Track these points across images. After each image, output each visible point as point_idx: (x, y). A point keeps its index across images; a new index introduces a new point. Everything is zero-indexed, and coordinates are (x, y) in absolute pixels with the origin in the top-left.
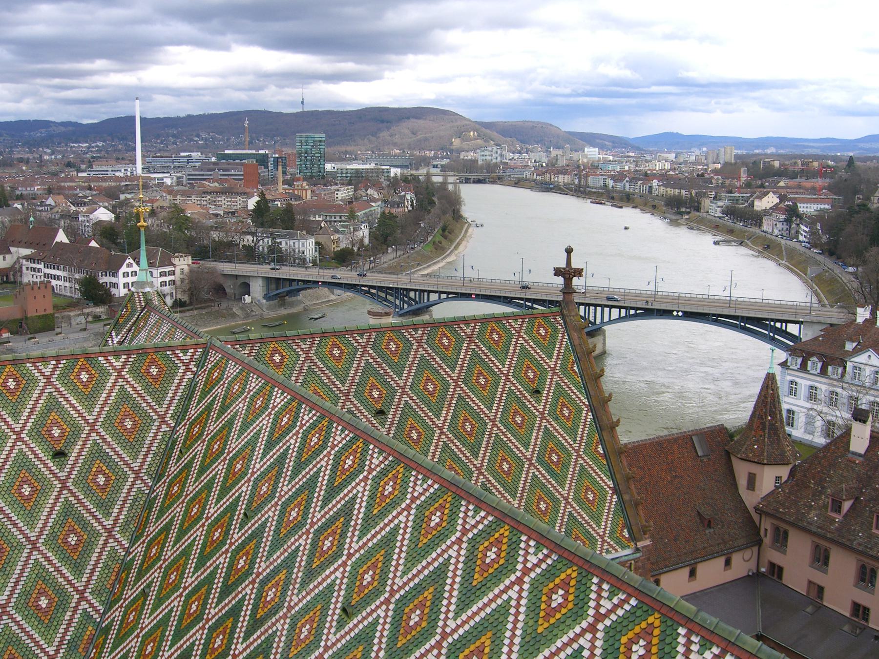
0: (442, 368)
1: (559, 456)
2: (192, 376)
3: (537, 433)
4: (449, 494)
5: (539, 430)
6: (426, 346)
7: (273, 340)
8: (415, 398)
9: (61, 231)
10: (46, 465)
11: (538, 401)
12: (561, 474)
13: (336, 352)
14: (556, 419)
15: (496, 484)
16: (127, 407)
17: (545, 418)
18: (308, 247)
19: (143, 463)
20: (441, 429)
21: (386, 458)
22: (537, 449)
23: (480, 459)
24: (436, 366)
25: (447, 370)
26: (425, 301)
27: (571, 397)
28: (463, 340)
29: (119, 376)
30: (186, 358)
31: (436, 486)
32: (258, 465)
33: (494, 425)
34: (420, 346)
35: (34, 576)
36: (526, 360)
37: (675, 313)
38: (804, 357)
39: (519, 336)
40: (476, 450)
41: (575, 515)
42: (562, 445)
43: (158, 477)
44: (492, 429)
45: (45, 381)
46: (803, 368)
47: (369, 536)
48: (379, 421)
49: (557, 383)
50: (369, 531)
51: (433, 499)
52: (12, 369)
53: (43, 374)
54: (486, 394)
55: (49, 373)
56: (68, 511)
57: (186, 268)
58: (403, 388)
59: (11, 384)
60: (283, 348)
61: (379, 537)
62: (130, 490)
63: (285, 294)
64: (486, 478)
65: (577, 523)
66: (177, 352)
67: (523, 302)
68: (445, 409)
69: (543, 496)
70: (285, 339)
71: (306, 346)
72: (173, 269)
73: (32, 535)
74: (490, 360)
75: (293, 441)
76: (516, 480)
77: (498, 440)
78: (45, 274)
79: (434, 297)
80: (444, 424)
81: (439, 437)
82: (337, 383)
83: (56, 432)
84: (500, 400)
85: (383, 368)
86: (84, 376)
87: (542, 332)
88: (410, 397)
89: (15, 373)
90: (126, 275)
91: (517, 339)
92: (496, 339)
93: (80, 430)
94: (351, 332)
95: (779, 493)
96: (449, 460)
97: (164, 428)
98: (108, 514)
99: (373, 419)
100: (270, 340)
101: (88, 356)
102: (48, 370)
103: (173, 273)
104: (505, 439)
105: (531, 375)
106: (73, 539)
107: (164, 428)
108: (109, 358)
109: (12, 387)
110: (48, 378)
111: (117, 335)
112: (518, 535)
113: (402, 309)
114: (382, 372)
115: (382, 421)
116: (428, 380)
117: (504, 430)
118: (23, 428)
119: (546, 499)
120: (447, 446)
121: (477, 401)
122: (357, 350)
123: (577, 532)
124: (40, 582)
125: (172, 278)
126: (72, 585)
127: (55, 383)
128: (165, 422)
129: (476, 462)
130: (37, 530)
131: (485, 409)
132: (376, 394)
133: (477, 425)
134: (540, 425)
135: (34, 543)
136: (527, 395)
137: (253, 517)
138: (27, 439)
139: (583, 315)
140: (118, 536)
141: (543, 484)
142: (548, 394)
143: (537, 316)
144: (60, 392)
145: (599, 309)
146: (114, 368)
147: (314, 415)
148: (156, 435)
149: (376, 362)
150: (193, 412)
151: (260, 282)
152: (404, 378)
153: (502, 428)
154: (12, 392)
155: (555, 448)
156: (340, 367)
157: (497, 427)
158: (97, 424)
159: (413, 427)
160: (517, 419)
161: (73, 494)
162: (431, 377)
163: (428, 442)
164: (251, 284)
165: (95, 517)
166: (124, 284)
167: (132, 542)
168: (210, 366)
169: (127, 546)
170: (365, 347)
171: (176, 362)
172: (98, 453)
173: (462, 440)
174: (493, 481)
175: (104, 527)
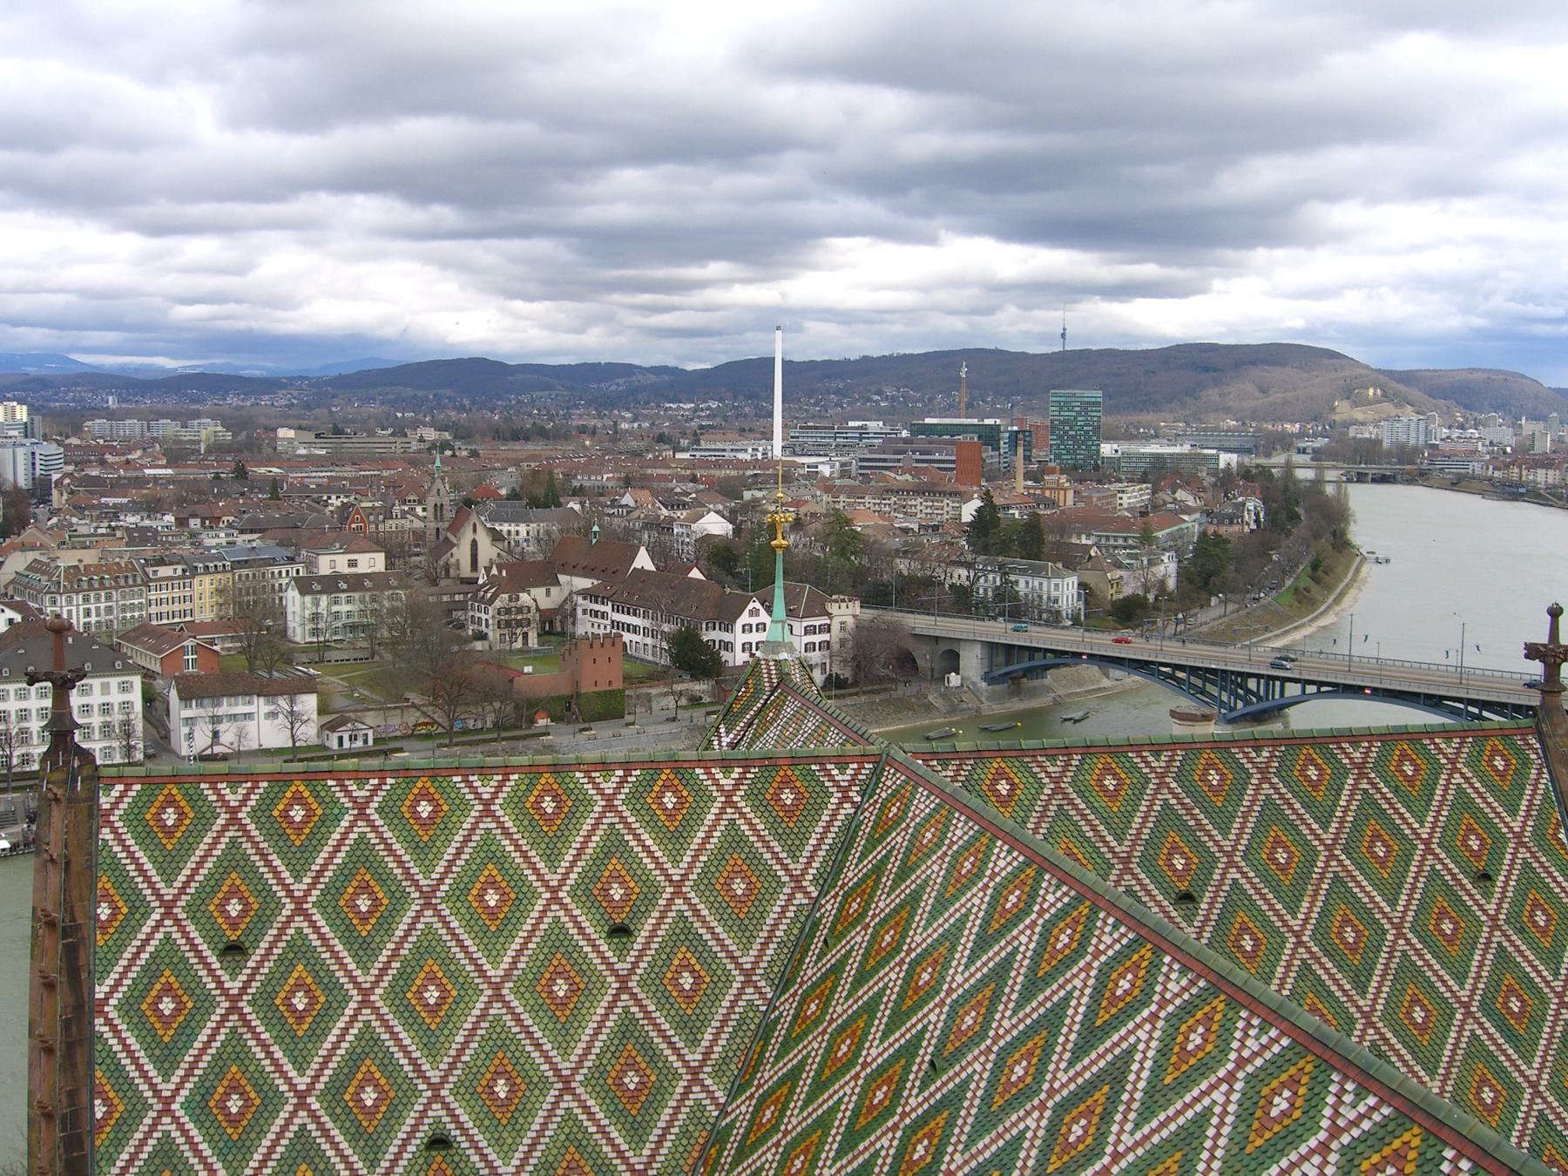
1: (1523, 1001)
2: (852, 811)
3: (1483, 956)
4: (1309, 1058)
5: (1485, 950)
6: (1275, 780)
7: (997, 754)
8: (1251, 874)
9: (643, 549)
10: (596, 948)
11: (1487, 895)
12: (1527, 1037)
13: (1110, 782)
14: (1521, 931)
15: (1398, 1046)
16: (738, 857)
17: (1499, 928)
18: (1065, 590)
19: (759, 957)
20: (1297, 935)
21: (1193, 983)
22: (1481, 986)
23: (1370, 996)
24: (1294, 817)
25: (1315, 826)
26: (1277, 696)
27: (1551, 891)
28: (1347, 771)
29: (729, 802)
30: (843, 779)
31: (1285, 1042)
32: (960, 978)
33: (1400, 935)
34: (1264, 779)
35: (563, 1137)
36: (1467, 815)
39: (1455, 769)
40: (1363, 979)
41: (1551, 1117)
42: (1531, 980)
43: (784, 983)
44: (1394, 942)
45: (604, 803)
47: (1154, 1124)
48: (1182, 913)
50: (1154, 1114)
51: (1277, 1064)
52: (551, 781)
53: (601, 792)
54: (1386, 876)
55: (611, 791)
56: (627, 1029)
57: (850, 621)
58: (1229, 855)
59: (548, 805)
60: (1015, 770)
61: (1173, 1127)
62: (734, 1003)
63: (1021, 674)
64: (1380, 1034)
65: (1553, 1134)
66: (829, 767)
67: (1462, 706)
68: (1307, 899)
69: (1490, 1076)
70: (1019, 753)
71: (1056, 769)
73: (565, 1067)
74: (1396, 811)
75: (1024, 939)
76: (1438, 1041)
77: (1407, 964)
79: (1292, 690)
80: (1303, 926)
81: (1294, 950)
82: (1109, 838)
83: (617, 893)
84: (1413, 888)
85: (1194, 817)
86: (669, 800)
87: (1499, 763)
88: (1242, 873)
89: (555, 786)
90: (747, 628)
91: (1450, 776)
92: (1410, 773)
93: (658, 891)
94: (1138, 748)
96: (1311, 995)
97: (800, 899)
98: (694, 1042)
99: (1171, 908)
100: (992, 754)
101: (677, 765)
102: (610, 785)
103: (828, 629)
104: (1420, 963)
105: (1474, 844)
106: (632, 1080)
107: (800, 899)
108: (713, 771)
109: (549, 810)
110: (609, 799)
111: (728, 733)
112: (1439, 1147)
113: (1232, 709)
114: (1192, 823)
115: (1189, 913)
116: (1277, 842)
117: (1419, 946)
118: (562, 883)
119: (1494, 1082)
120: (1308, 967)
121: (1369, 888)
122: (1148, 781)
123: (1554, 1152)
124: (572, 1150)
125: (825, 637)
126: (625, 1160)
127: (620, 809)
128: (801, 888)
129: (1361, 1003)
130: (574, 1058)
131: (1383, 904)
132: (1179, 863)
133: (1366, 933)
134: (1489, 941)
135: (567, 1081)
136: (1465, 881)
137: (945, 1070)
138: (568, 900)
140: (709, 1082)
141: (1490, 1053)
142: (1506, 883)
143: (1489, 733)
144: (627, 825)
146: (721, 789)
147: (1065, 894)
148: (784, 909)
149: (1182, 804)
150: (851, 875)
151: (977, 651)
152: (1232, 837)
153: (1415, 941)
154: (549, 820)
155: (1517, 987)
156: (1115, 809)
157: (1406, 939)
158: (687, 883)
159: (1244, 929)
160: (1444, 927)
161: (638, 1002)
162: (1284, 839)
163: (1272, 958)
164: (961, 653)
165: (671, 1044)
167: (733, 1095)
168: (884, 795)
169: (722, 1100)
170: (1161, 776)
171: (827, 784)
172: (684, 934)
173: (1338, 958)
174: (1394, 1041)
175: (686, 1063)
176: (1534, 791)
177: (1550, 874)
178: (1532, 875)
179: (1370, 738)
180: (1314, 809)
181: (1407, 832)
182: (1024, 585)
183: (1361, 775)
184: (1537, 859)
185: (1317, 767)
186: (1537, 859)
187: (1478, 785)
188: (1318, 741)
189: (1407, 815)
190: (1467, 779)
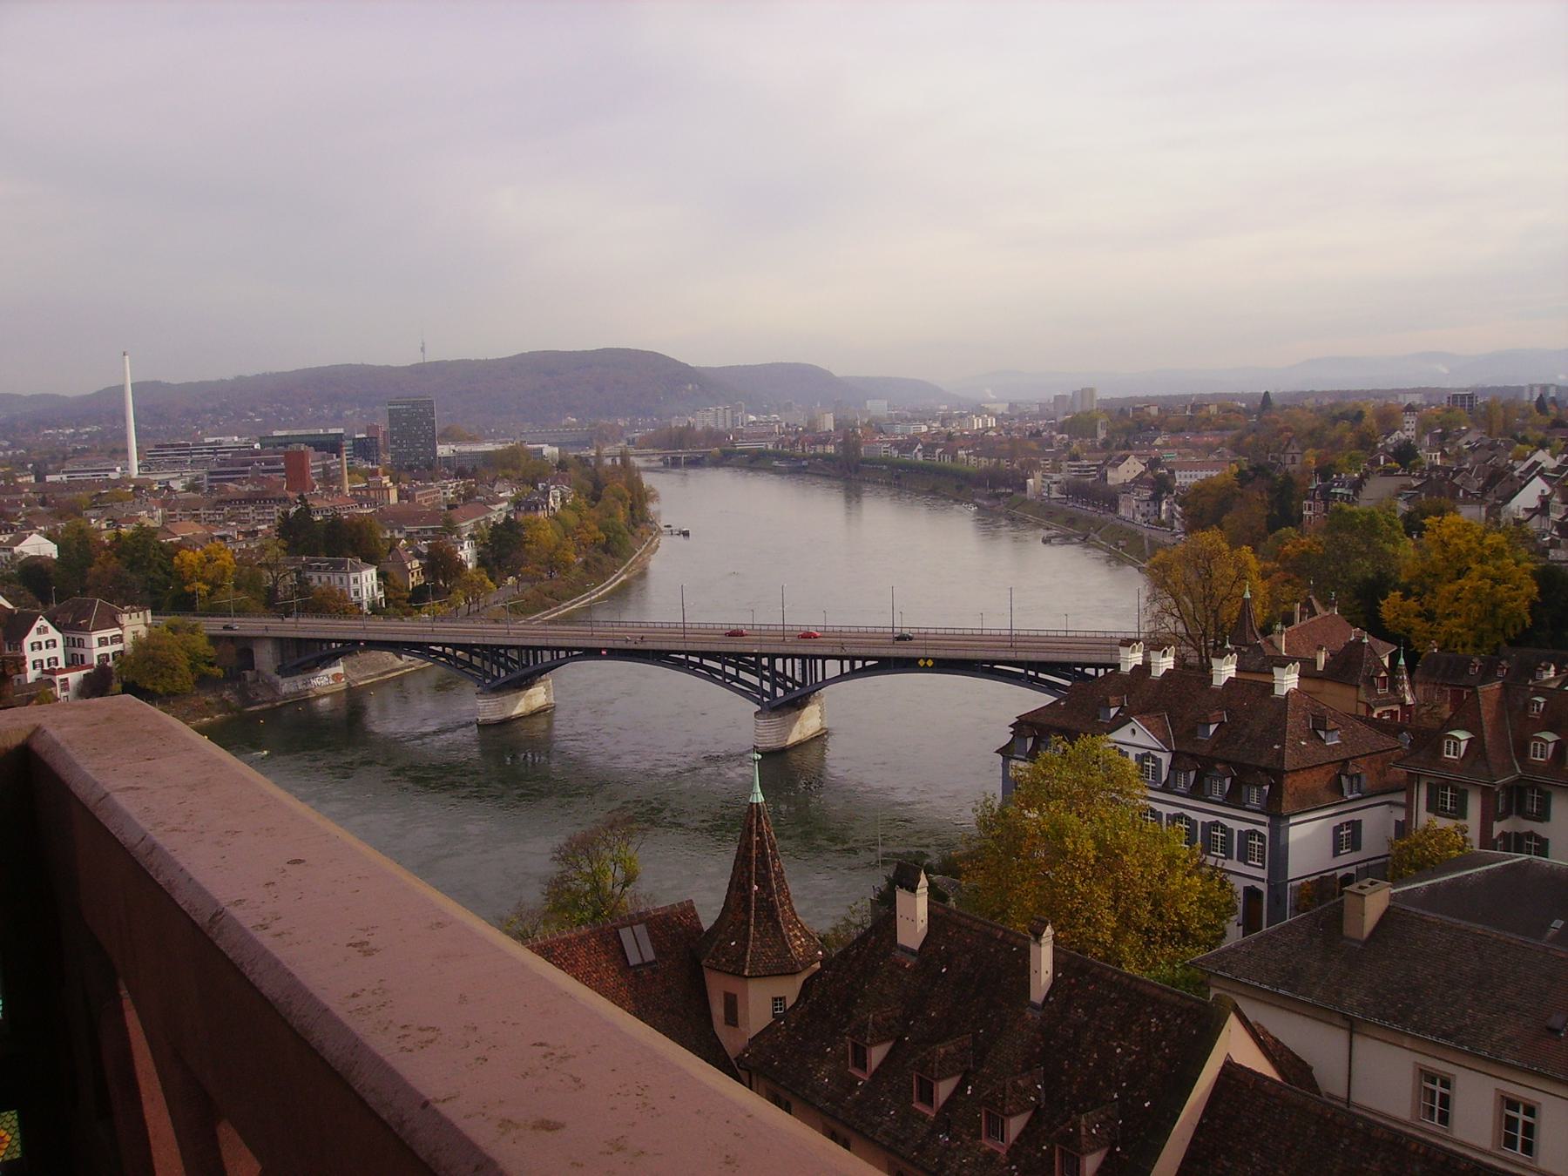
18: (366, 582)
26: (540, 662)
37: (921, 663)
38: (1035, 737)
57: (143, 631)
67: (683, 657)
72: (120, 632)
95: (779, 1029)
103: (120, 639)
113: (495, 678)
125: (118, 647)
139: (781, 671)
145: (819, 662)
164: (255, 650)
166: (34, 662)
182: (317, 580)
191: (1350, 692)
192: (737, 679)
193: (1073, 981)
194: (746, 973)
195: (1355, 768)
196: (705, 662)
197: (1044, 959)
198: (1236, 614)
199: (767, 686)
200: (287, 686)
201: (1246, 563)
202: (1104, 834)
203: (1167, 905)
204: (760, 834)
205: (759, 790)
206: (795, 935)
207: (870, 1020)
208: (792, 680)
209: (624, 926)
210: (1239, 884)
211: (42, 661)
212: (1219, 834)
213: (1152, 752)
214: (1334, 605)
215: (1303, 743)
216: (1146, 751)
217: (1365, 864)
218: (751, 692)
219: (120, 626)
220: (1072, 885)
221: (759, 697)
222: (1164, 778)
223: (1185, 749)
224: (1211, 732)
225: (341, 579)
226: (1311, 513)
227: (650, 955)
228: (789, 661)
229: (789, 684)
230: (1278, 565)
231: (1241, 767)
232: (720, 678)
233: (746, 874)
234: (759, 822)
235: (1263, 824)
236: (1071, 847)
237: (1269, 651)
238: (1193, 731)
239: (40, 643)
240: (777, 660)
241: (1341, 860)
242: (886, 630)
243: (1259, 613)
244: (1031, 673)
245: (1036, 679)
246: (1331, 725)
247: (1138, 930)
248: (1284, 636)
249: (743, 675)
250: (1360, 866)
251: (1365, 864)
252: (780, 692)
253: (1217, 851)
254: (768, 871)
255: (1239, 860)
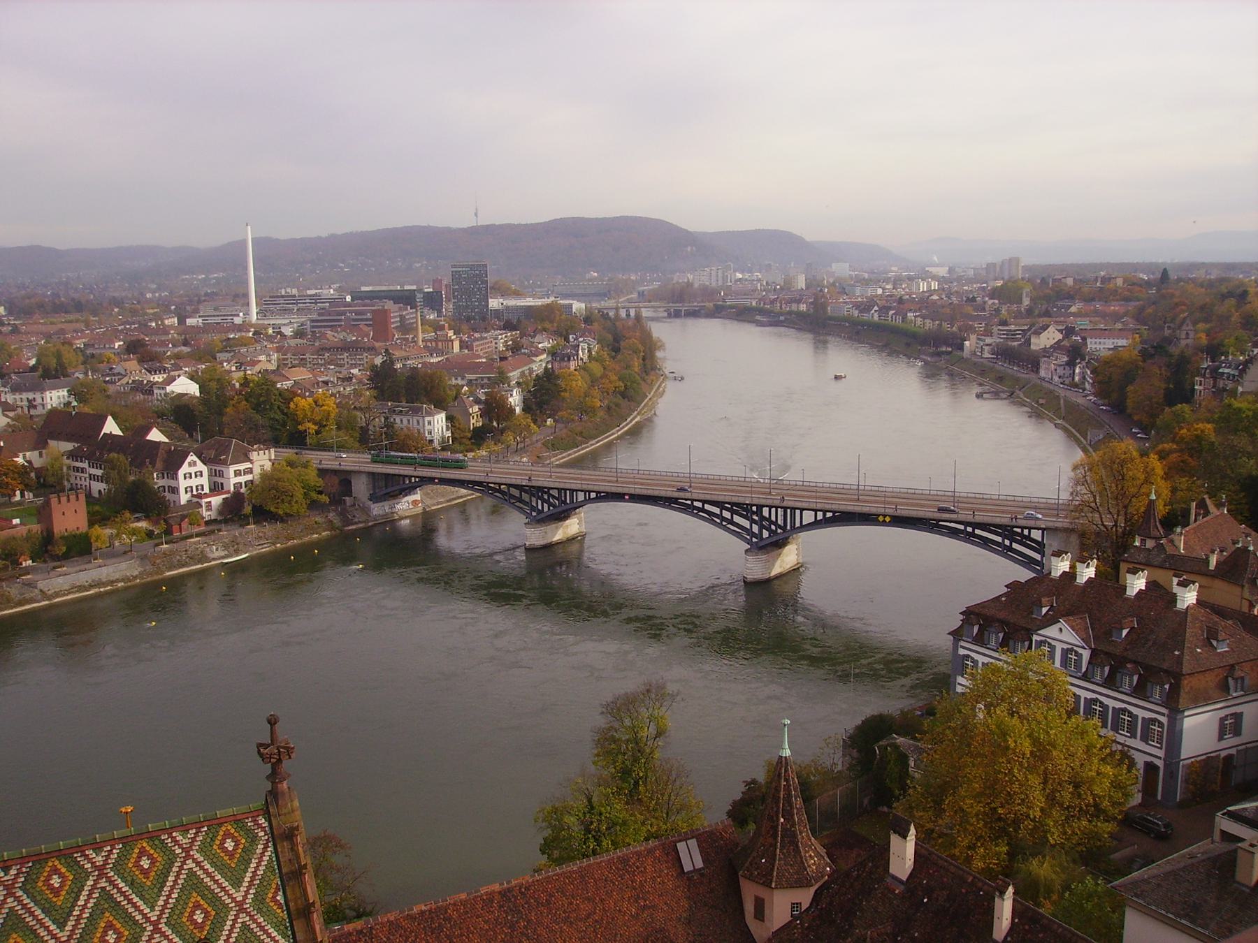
0: (42, 925)
6: (20, 893)
9: (110, 418)
18: (437, 425)
25: (53, 927)
28: (88, 875)
36: (195, 894)
38: (980, 624)
39: (188, 856)
46: (980, 640)
49: (245, 926)
57: (268, 466)
63: (398, 492)
67: (689, 502)
72: (251, 466)
74: (130, 901)
78: (90, 475)
87: (229, 845)
91: (184, 863)
95: (795, 927)
103: (250, 471)
105: (199, 917)
125: (249, 477)
139: (768, 516)
143: (222, 820)
166: (186, 488)
176: (259, 864)
177: (266, 932)
178: (249, 935)
179: (113, 842)
180: (54, 913)
181: (138, 917)
182: (402, 422)
183: (100, 877)
184: (255, 921)
185: (61, 875)
186: (255, 921)
187: (208, 866)
188: (63, 852)
189: (140, 903)
190: (198, 863)
191: (1237, 590)
192: (731, 522)
193: (1027, 927)
194: (773, 886)
195: (1240, 672)
196: (707, 507)
197: (1005, 909)
198: (1142, 509)
199: (755, 529)
200: (377, 509)
201: (1153, 469)
202: (1039, 734)
203: (1084, 788)
204: (787, 780)
205: (787, 747)
206: (810, 855)
207: (868, 936)
208: (775, 523)
209: (680, 841)
210: (1140, 760)
211: (192, 487)
212: (1126, 718)
213: (1075, 648)
214: (1224, 506)
215: (1199, 650)
216: (1070, 646)
217: (1244, 747)
218: (741, 533)
219: (251, 461)
220: (1011, 770)
221: (748, 537)
222: (1084, 669)
223: (1101, 647)
224: (1124, 635)
225: (418, 422)
226: (1201, 388)
227: (699, 864)
228: (773, 510)
229: (773, 527)
230: (1175, 447)
231: (1147, 668)
232: (718, 521)
233: (775, 809)
234: (786, 771)
235: (1163, 714)
236: (1013, 745)
237: (1170, 550)
238: (1109, 633)
239: (191, 474)
240: (764, 509)
241: (1224, 744)
242: (852, 487)
243: (1161, 510)
244: (969, 529)
245: (973, 534)
246: (1222, 635)
247: (1061, 805)
248: (1183, 537)
249: (737, 519)
250: (1240, 748)
251: (1244, 747)
252: (766, 534)
253: (1124, 730)
254: (792, 807)
255: (1141, 740)
